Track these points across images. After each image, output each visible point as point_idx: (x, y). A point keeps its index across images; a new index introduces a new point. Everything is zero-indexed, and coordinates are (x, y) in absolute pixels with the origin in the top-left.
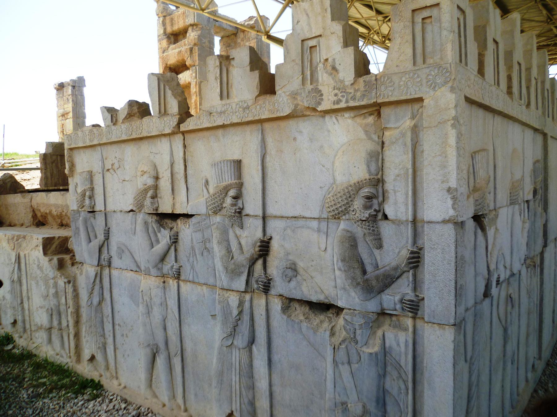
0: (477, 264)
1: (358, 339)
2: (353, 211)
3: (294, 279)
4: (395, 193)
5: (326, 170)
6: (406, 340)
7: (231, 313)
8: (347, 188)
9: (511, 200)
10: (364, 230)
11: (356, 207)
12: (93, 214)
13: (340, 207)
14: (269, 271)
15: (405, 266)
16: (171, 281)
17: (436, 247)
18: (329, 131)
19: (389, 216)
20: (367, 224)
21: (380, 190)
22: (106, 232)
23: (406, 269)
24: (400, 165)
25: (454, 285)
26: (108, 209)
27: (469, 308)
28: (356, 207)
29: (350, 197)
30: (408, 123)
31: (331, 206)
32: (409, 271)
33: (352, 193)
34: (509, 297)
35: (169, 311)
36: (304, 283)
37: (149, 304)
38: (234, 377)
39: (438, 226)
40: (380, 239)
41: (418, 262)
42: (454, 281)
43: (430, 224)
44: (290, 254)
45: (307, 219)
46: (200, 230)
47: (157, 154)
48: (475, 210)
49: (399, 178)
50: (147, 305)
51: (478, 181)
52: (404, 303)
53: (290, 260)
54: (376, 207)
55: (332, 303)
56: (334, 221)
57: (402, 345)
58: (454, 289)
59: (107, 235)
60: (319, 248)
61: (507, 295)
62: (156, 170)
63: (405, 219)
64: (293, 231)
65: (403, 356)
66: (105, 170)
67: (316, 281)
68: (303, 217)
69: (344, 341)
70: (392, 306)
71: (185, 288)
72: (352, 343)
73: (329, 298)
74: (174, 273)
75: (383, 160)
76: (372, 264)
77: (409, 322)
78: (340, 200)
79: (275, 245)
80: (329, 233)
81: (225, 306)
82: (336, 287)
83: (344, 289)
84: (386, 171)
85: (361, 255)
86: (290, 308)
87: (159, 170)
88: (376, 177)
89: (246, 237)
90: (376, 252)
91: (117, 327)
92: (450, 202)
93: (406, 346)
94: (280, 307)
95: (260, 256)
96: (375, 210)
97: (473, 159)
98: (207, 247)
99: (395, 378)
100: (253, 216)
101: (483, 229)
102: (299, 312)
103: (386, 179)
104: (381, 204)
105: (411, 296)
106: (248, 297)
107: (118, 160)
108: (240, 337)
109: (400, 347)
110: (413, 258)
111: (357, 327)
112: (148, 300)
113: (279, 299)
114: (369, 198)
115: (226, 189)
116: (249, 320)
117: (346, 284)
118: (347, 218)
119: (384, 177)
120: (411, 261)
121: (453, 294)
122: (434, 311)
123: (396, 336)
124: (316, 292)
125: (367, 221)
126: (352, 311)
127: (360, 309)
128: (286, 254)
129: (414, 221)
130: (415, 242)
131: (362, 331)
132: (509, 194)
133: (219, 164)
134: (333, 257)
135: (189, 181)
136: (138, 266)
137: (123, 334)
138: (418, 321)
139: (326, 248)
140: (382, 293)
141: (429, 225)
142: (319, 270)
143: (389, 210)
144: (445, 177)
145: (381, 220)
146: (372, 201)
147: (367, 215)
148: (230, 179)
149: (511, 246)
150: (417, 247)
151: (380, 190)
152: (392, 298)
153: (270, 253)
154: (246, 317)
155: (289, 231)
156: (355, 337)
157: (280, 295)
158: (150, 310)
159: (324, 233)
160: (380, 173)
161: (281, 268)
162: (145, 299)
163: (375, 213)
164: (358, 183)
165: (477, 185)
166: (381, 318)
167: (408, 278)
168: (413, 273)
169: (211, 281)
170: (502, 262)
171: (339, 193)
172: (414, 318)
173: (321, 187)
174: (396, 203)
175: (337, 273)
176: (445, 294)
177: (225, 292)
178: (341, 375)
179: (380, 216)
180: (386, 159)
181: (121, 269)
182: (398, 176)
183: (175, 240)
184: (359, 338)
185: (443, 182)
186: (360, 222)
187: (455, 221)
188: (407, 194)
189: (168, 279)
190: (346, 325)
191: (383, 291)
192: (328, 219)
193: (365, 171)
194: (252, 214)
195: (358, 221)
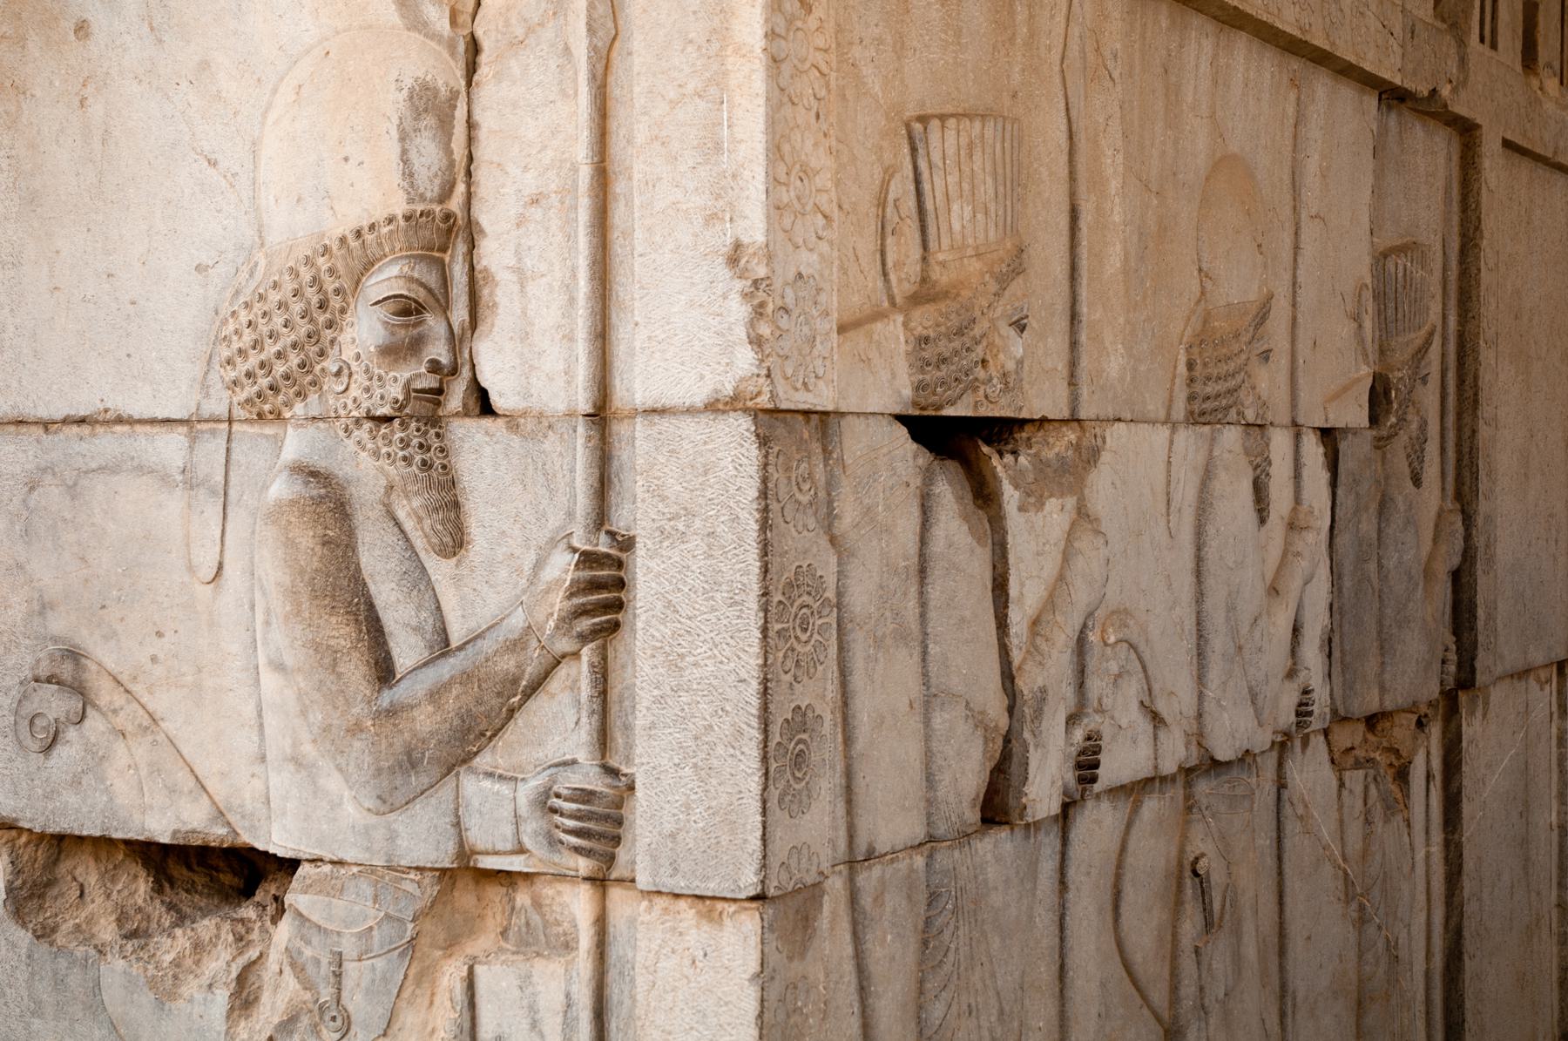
0: (933, 649)
2: (338, 374)
8: (308, 261)
9: (1191, 398)
10: (384, 462)
11: (348, 354)
13: (279, 355)
15: (557, 627)
17: (681, 527)
19: (497, 401)
20: (399, 435)
21: (459, 273)
23: (564, 645)
24: (545, 148)
25: (755, 702)
27: (881, 848)
28: (348, 354)
29: (323, 306)
31: (240, 351)
32: (576, 655)
34: (1188, 873)
39: (690, 428)
40: (456, 505)
41: (619, 606)
42: (755, 685)
43: (656, 418)
45: (138, 428)
48: (920, 387)
49: (536, 213)
51: (941, 257)
52: (554, 811)
54: (439, 351)
55: (247, 838)
56: (254, 430)
58: (755, 722)
60: (191, 569)
61: (1180, 865)
63: (561, 407)
68: (120, 420)
73: (231, 818)
75: (471, 125)
76: (417, 629)
77: (578, 904)
78: (278, 321)
80: (232, 493)
83: (297, 761)
85: (372, 588)
88: (437, 208)
90: (439, 569)
92: (738, 311)
96: (435, 367)
97: (914, 150)
101: (983, 495)
103: (483, 216)
105: (588, 777)
110: (595, 586)
111: (348, 947)
114: (408, 309)
117: (305, 736)
120: (583, 600)
121: (754, 744)
122: (673, 836)
126: (327, 868)
127: (362, 857)
129: (601, 416)
130: (601, 517)
132: (1182, 368)
134: (253, 607)
138: (616, 894)
139: (220, 567)
140: (462, 769)
141: (652, 424)
142: (189, 678)
144: (718, 197)
145: (466, 413)
146: (420, 323)
147: (396, 392)
149: (1198, 624)
150: (612, 534)
151: (459, 273)
152: (505, 789)
159: (213, 492)
160: (461, 188)
163: (430, 382)
164: (358, 234)
165: (936, 273)
166: (465, 898)
167: (574, 687)
168: (596, 660)
170: (1132, 689)
171: (275, 285)
172: (600, 882)
173: (198, 268)
176: (720, 750)
179: (456, 396)
182: (535, 201)
185: (712, 218)
186: (368, 425)
187: (764, 401)
188: (569, 289)
190: (299, 943)
191: (467, 759)
192: (230, 421)
195: (358, 421)
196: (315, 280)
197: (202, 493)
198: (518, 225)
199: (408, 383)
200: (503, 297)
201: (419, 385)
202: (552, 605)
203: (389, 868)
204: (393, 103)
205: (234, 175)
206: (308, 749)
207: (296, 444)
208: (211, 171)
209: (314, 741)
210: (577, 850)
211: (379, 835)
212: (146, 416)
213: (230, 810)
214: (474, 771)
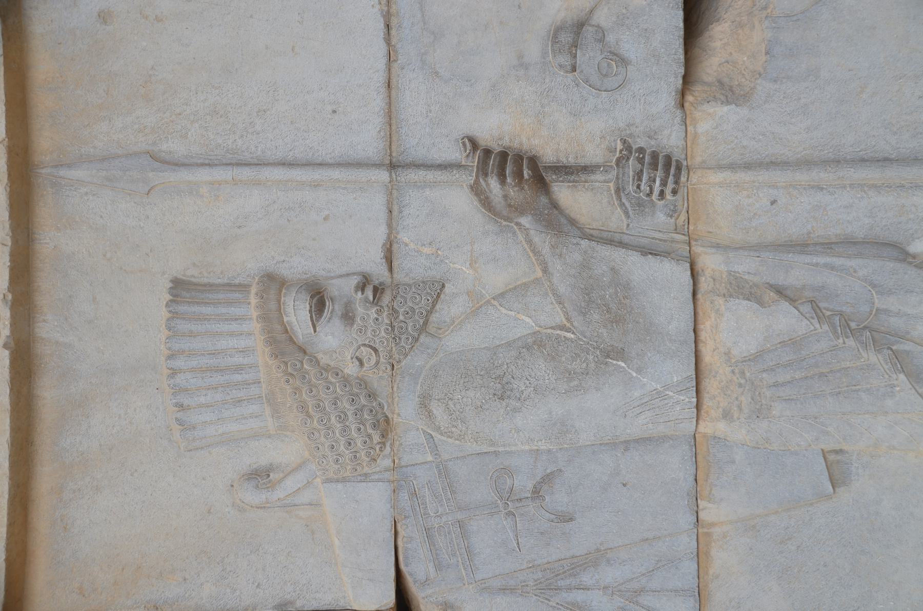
14: (594, 153)
44: (520, 57)
46: (461, 524)
86: (726, 80)
89: (473, 263)
94: (726, 108)
95: (540, 183)
98: (530, 486)
100: (390, 226)
116: (808, 259)
133: (180, 379)
153: (525, 147)
177: (711, 386)
194: (381, 232)
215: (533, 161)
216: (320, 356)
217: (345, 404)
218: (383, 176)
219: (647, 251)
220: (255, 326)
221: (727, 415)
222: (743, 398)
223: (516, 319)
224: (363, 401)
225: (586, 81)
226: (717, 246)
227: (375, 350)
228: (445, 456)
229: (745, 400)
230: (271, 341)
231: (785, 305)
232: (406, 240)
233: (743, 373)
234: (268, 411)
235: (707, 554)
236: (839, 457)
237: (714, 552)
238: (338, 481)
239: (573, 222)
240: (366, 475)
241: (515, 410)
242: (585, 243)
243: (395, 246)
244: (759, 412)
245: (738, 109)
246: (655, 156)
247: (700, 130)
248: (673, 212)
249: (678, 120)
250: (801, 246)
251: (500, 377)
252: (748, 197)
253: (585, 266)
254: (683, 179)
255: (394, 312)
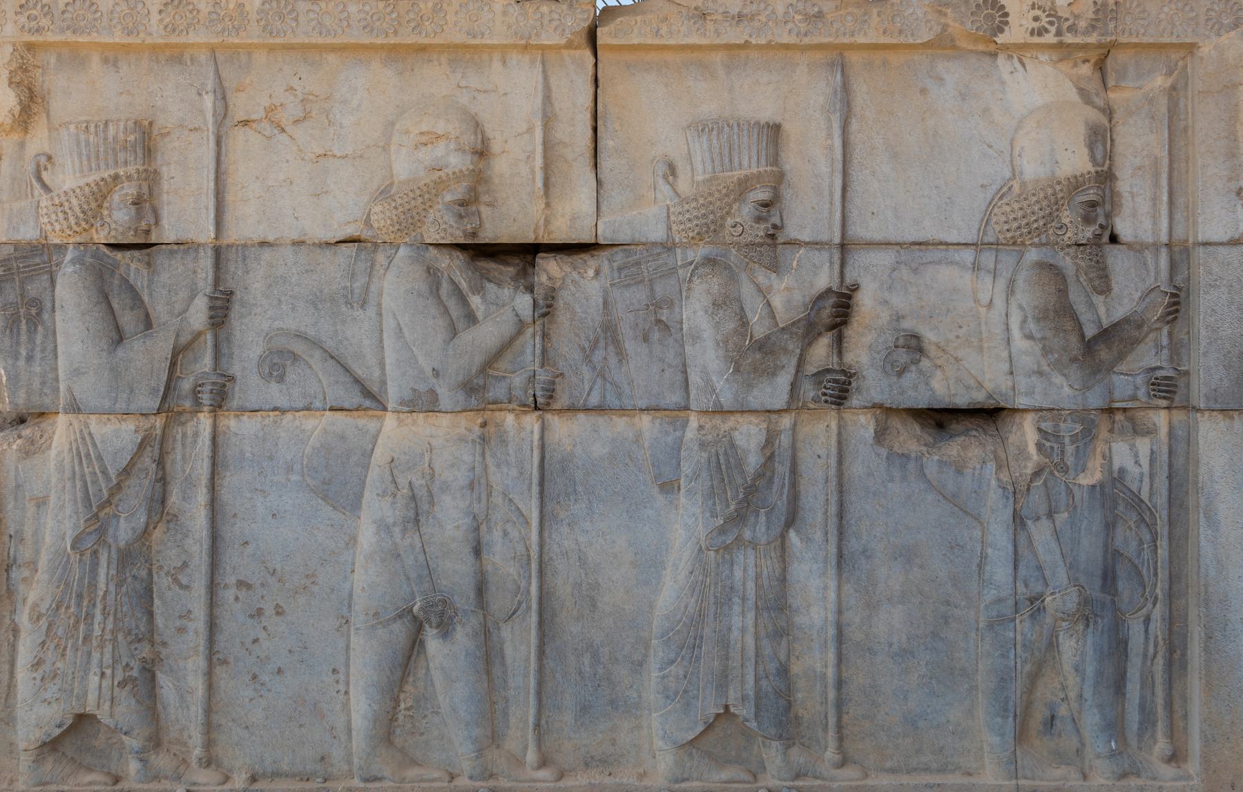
1: (1069, 463)
3: (913, 368)
4: (1133, 198)
5: (996, 155)
6: (1152, 450)
7: (740, 464)
12: (145, 251)
13: (1036, 221)
14: (849, 358)
16: (510, 419)
18: (1003, 83)
22: (219, 303)
24: (1143, 150)
26: (233, 234)
28: (1066, 221)
30: (1159, 81)
33: (1059, 196)
35: (498, 499)
36: (939, 373)
37: (422, 493)
38: (736, 621)
40: (1107, 277)
44: (903, 317)
47: (485, 91)
50: (413, 497)
52: (1153, 384)
53: (905, 330)
57: (1145, 462)
59: (220, 313)
60: (976, 301)
62: (479, 131)
63: (1151, 240)
64: (915, 271)
65: (1146, 480)
66: (228, 122)
67: (966, 366)
68: (941, 243)
69: (1037, 474)
70: (1129, 391)
71: (564, 430)
72: (1056, 473)
73: (995, 396)
74: (539, 393)
75: (1112, 140)
78: (1036, 208)
79: (866, 301)
81: (721, 451)
82: (1012, 373)
83: (1040, 373)
84: (1118, 160)
85: (1075, 307)
87: (489, 134)
89: (787, 289)
90: (1098, 300)
91: (228, 595)
93: (1152, 461)
94: (872, 431)
95: (832, 327)
96: (1101, 226)
98: (664, 318)
99: (1131, 523)
100: (807, 244)
102: (909, 438)
104: (1108, 216)
106: (786, 421)
107: (300, 97)
108: (763, 518)
109: (1140, 465)
111: (1067, 440)
112: (418, 482)
113: (869, 416)
115: (744, 186)
117: (1044, 362)
118: (1044, 241)
119: (1114, 169)
120: (1169, 310)
123: (1132, 447)
124: (968, 388)
125: (1088, 247)
128: (894, 318)
131: (1077, 447)
135: (606, 163)
136: (367, 394)
137: (260, 612)
143: (1124, 228)
148: (754, 164)
152: (1130, 378)
154: (782, 469)
155: (905, 273)
156: (1062, 459)
157: (875, 406)
158: (425, 507)
159: (989, 271)
161: (880, 348)
162: (402, 481)
169: (674, 398)
173: (982, 186)
174: (1134, 215)
175: (1019, 342)
177: (717, 420)
178: (1031, 542)
180: (1118, 140)
181: (275, 409)
183: (546, 310)
184: (1070, 460)
189: (503, 413)
193: (1086, 158)
195: (1069, 246)
196: (1054, 194)
197: (982, 273)
198: (1132, 177)
199: (1094, 232)
200: (1127, 204)
201: (1096, 233)
202: (1157, 311)
203: (1083, 410)
204: (1082, 130)
205: (1002, 152)
206: (1046, 368)
207: (1033, 255)
208: (991, 150)
209: (1049, 365)
210: (1165, 398)
211: (1080, 398)
212: (955, 242)
213: (995, 393)
214: (1114, 372)
215: (845, 323)
216: (737, 204)
217: (711, 217)
218: (837, 240)
219: (794, 386)
220: (754, 170)
221: (701, 427)
222: (710, 436)
223: (757, 312)
224: (712, 228)
225: (889, 353)
226: (795, 425)
227: (740, 235)
228: (680, 271)
229: (710, 438)
230: (747, 179)
231: (762, 460)
232: (801, 252)
233: (725, 436)
234: (707, 176)
235: (624, 415)
236: (676, 488)
237: (624, 418)
238: (668, 213)
239: (810, 344)
240: (671, 229)
241: (706, 312)
242: (798, 351)
243: (797, 246)
244: (703, 445)
245: (872, 438)
246: (847, 391)
247: (860, 416)
248: (814, 400)
249: (867, 405)
250: (794, 470)
251: (725, 303)
252: (823, 443)
253: (786, 351)
254: (833, 407)
255: (761, 245)
